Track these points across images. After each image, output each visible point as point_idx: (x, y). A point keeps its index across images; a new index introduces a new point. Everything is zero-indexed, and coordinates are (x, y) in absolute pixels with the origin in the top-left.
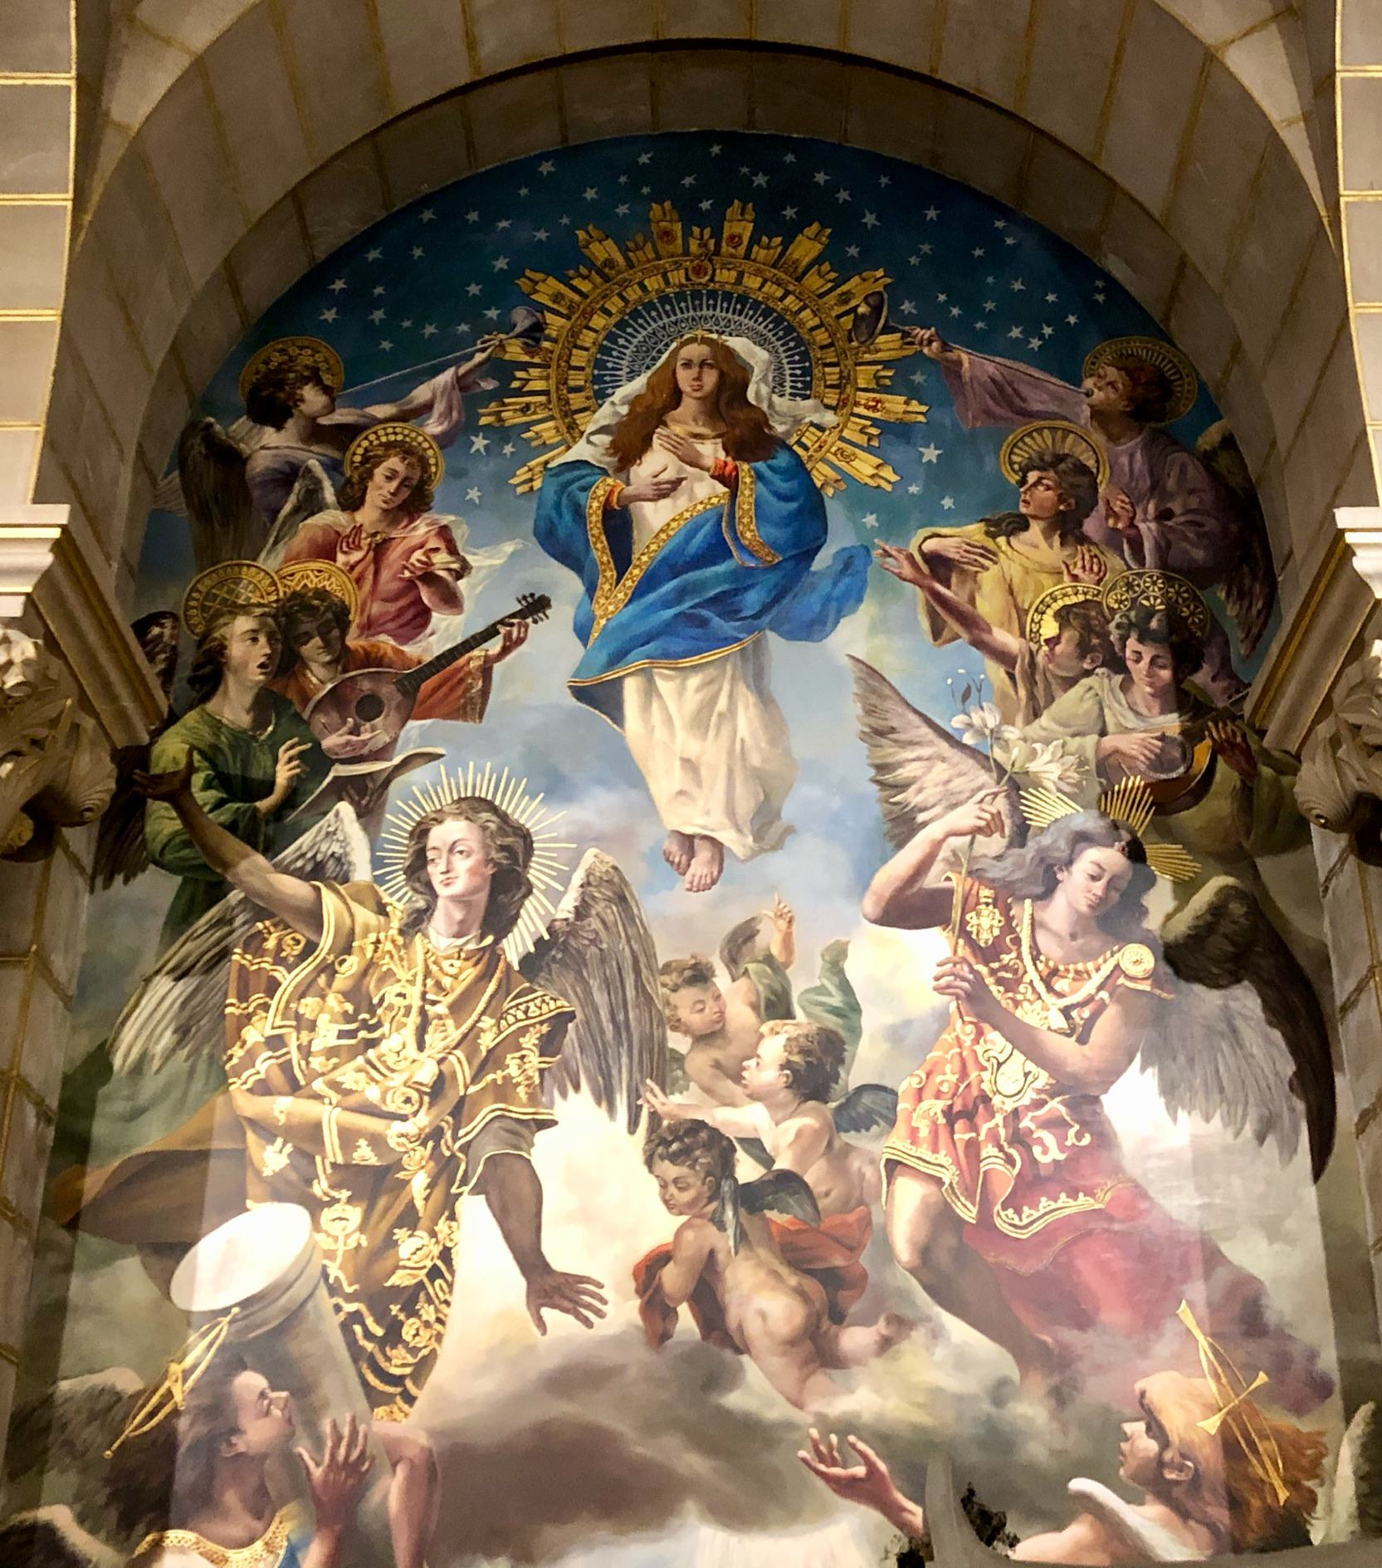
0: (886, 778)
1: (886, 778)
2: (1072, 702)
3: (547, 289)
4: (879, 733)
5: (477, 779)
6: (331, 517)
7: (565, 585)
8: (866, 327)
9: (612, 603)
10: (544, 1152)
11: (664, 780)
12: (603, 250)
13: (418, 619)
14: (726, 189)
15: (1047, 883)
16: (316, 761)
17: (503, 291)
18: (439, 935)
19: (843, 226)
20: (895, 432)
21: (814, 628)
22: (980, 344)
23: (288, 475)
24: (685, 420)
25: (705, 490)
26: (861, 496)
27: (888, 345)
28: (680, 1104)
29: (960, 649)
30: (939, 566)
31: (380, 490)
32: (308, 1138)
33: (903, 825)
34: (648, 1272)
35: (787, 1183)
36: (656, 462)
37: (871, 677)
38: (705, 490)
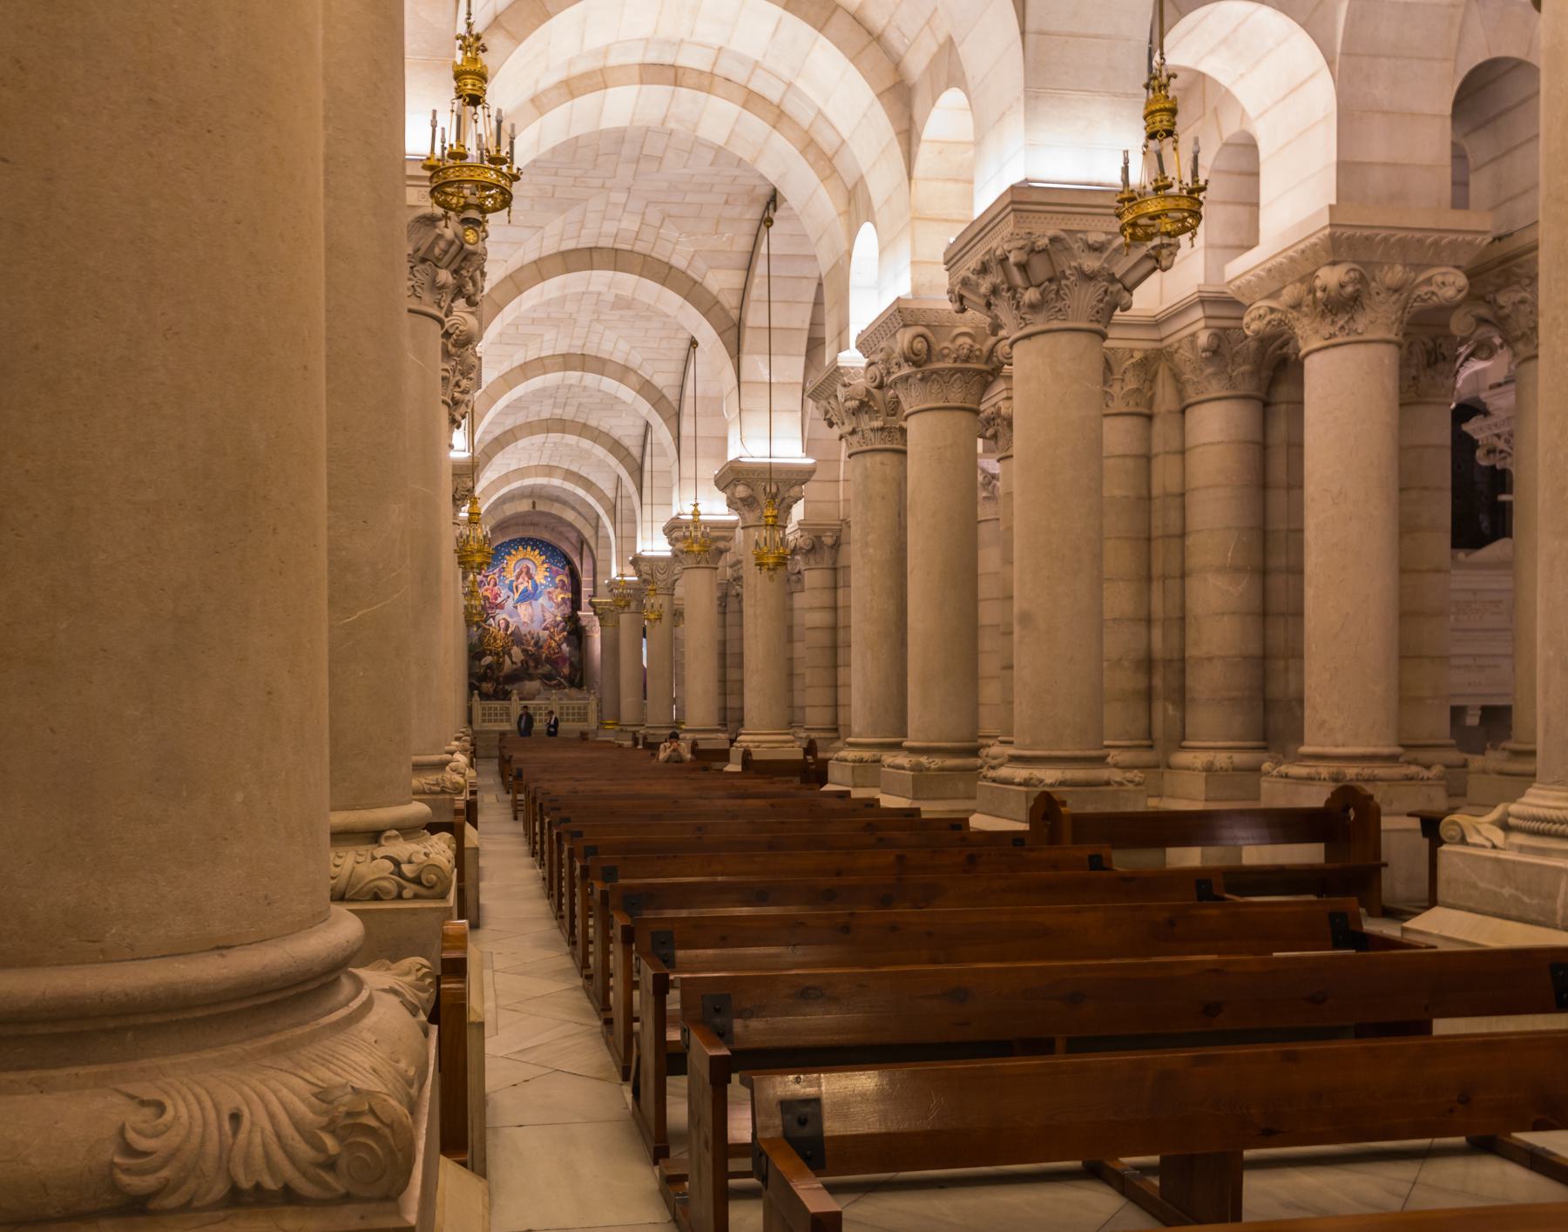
0: (544, 616)
1: (544, 616)
2: (562, 608)
3: (508, 557)
4: (543, 611)
5: (504, 616)
6: (487, 587)
7: (511, 594)
8: (543, 563)
9: (517, 596)
10: (512, 652)
11: (522, 616)
12: (514, 552)
13: (496, 599)
14: (528, 544)
15: (558, 626)
16: (488, 614)
17: (503, 558)
18: (501, 632)
19: (540, 549)
20: (546, 577)
21: (536, 600)
22: (556, 566)
23: (482, 581)
24: (523, 575)
25: (526, 584)
26: (542, 584)
27: (545, 566)
28: (524, 647)
29: (551, 602)
30: (549, 593)
31: (492, 583)
32: (491, 651)
33: (545, 621)
34: (522, 662)
35: (533, 654)
36: (520, 580)
37: (542, 606)
38: (526, 584)
